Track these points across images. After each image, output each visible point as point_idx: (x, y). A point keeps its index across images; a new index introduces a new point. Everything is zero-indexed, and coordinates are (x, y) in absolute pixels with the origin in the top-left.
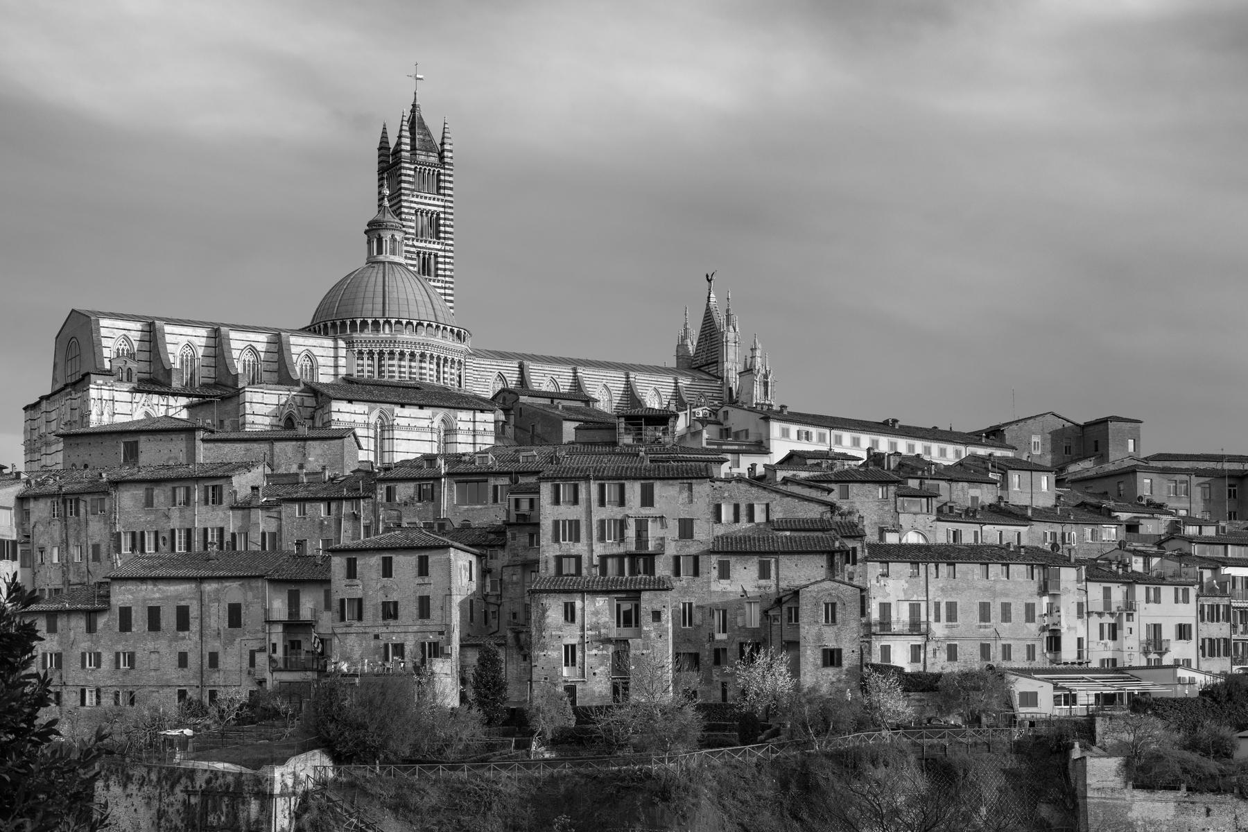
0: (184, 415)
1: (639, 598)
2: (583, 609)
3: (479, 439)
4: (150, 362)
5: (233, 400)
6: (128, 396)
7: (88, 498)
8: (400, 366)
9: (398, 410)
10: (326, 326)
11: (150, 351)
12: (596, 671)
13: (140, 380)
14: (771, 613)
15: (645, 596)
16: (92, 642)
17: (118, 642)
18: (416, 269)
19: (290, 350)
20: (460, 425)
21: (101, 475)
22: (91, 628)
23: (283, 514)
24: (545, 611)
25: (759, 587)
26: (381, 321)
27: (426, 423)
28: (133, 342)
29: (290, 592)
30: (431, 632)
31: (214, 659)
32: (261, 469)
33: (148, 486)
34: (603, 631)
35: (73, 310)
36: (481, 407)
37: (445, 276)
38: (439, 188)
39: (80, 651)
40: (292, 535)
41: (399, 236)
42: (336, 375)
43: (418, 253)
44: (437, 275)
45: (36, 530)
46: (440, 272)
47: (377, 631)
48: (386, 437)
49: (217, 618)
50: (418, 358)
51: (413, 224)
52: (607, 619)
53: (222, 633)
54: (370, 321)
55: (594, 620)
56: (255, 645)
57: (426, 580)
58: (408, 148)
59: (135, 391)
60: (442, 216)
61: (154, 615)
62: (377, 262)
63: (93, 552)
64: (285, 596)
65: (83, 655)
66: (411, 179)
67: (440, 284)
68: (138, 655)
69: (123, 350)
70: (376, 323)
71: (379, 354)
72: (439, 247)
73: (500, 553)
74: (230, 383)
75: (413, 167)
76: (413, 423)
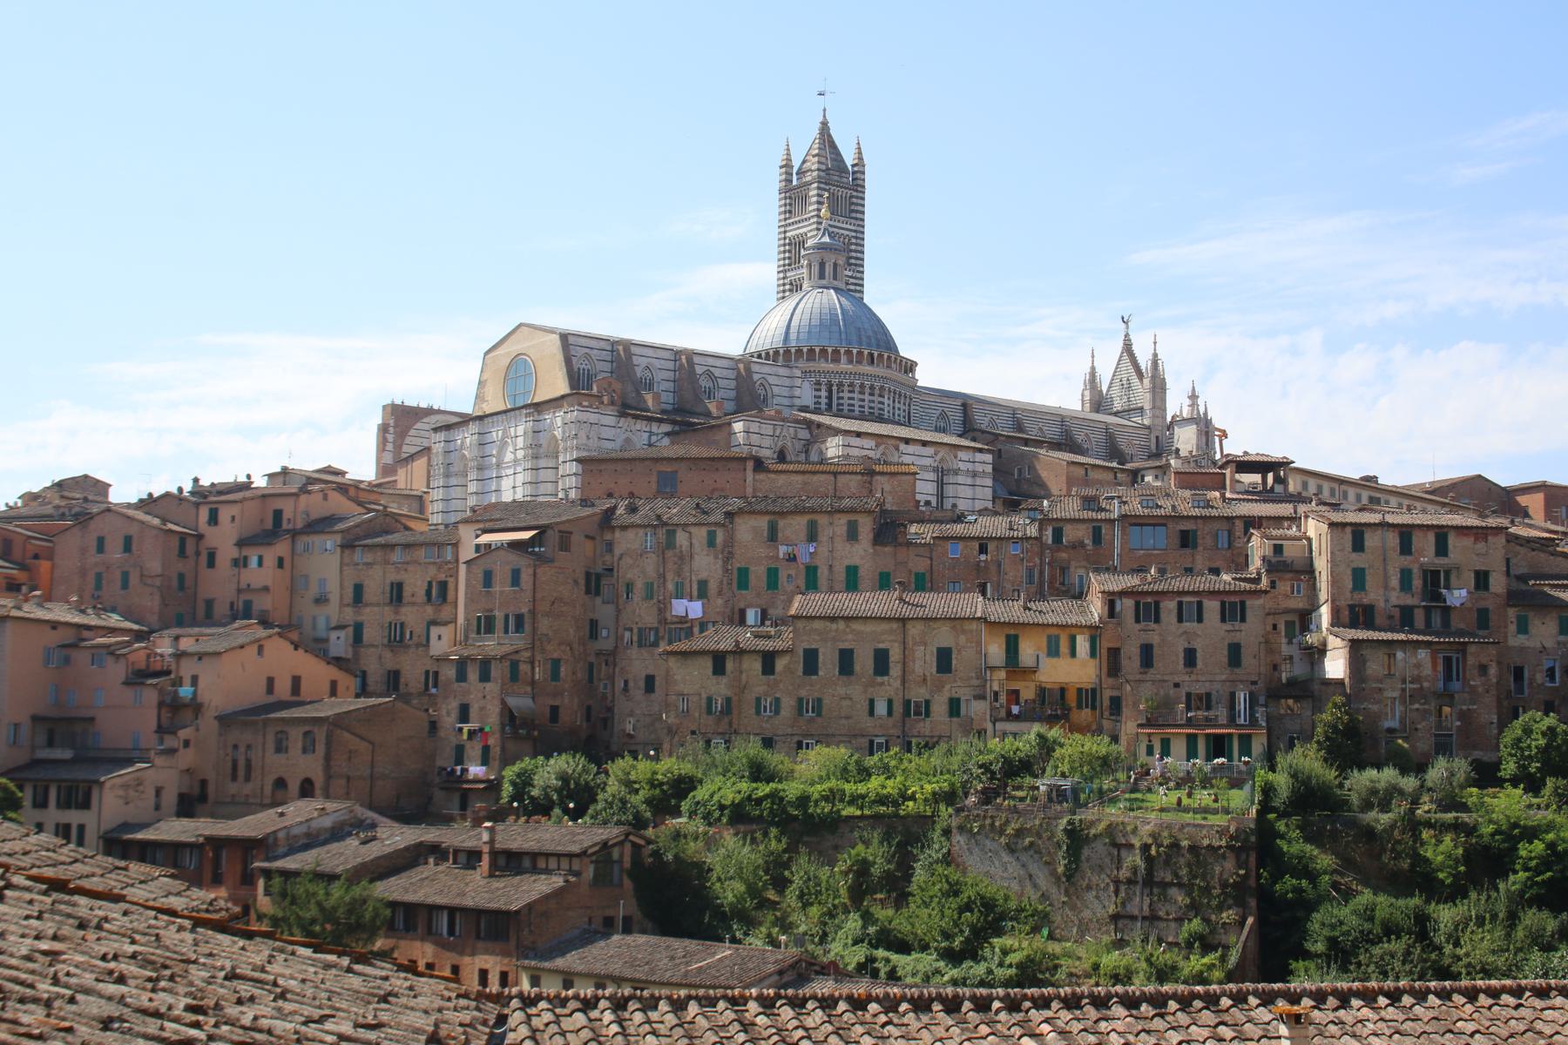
1: (1464, 652)
6: (611, 420)
7: (693, 530)
9: (902, 447)
15: (1472, 649)
24: (1364, 662)
27: (928, 462)
29: (1008, 637)
30: (1241, 681)
33: (772, 517)
35: (520, 325)
47: (1177, 680)
49: (924, 661)
50: (877, 392)
55: (1416, 672)
59: (623, 415)
61: (846, 661)
63: (699, 589)
64: (1003, 640)
65: (758, 700)
68: (826, 701)
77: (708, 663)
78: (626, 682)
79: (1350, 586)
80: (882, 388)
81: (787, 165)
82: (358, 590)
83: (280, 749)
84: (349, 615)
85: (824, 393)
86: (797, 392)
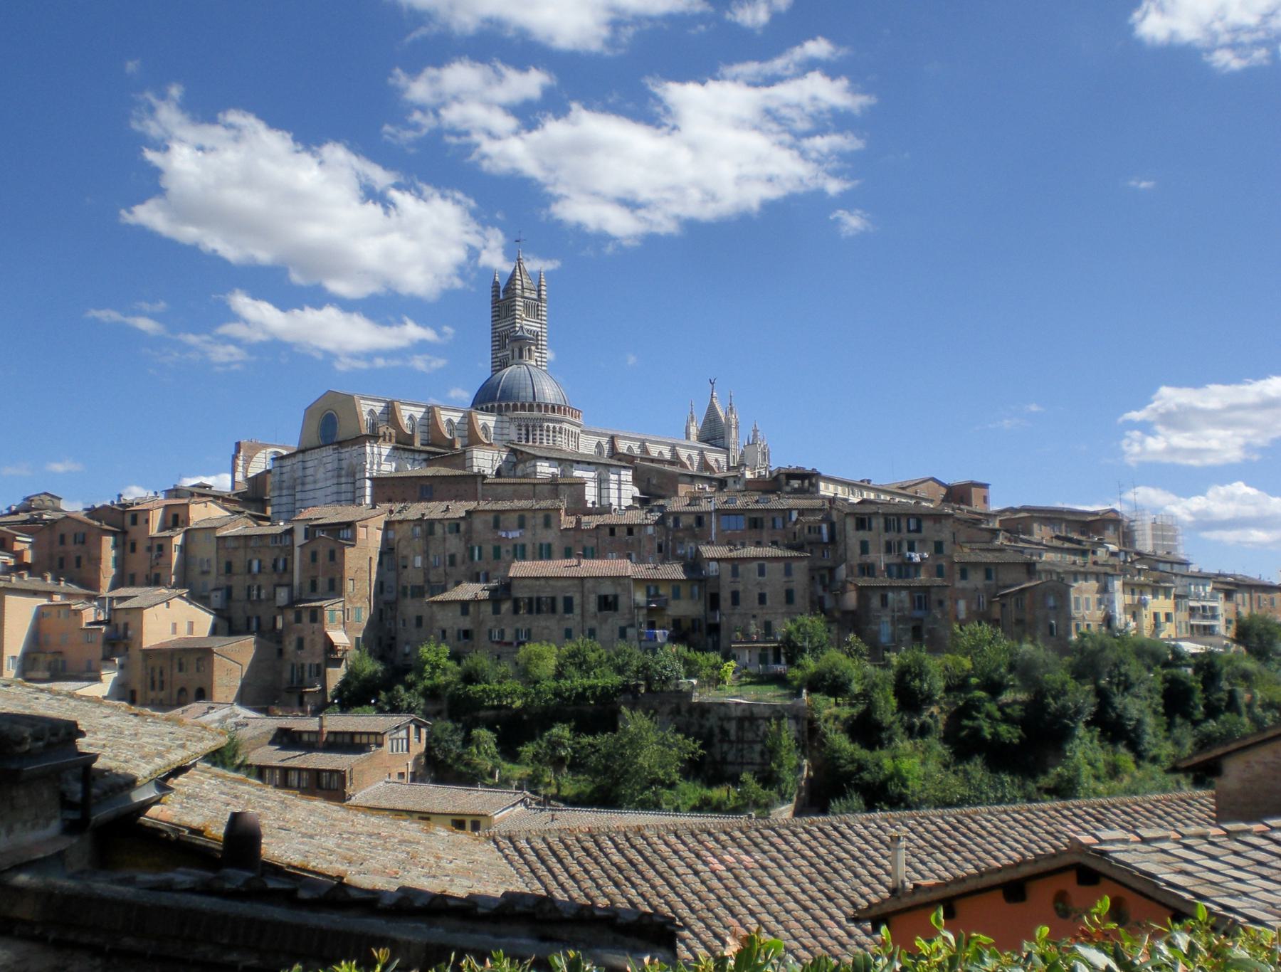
45: (401, 544)
47: (755, 612)
77: (458, 608)
78: (404, 620)
81: (496, 286)
82: (229, 566)
83: (181, 670)
84: (223, 581)
85: (523, 432)
86: (506, 431)
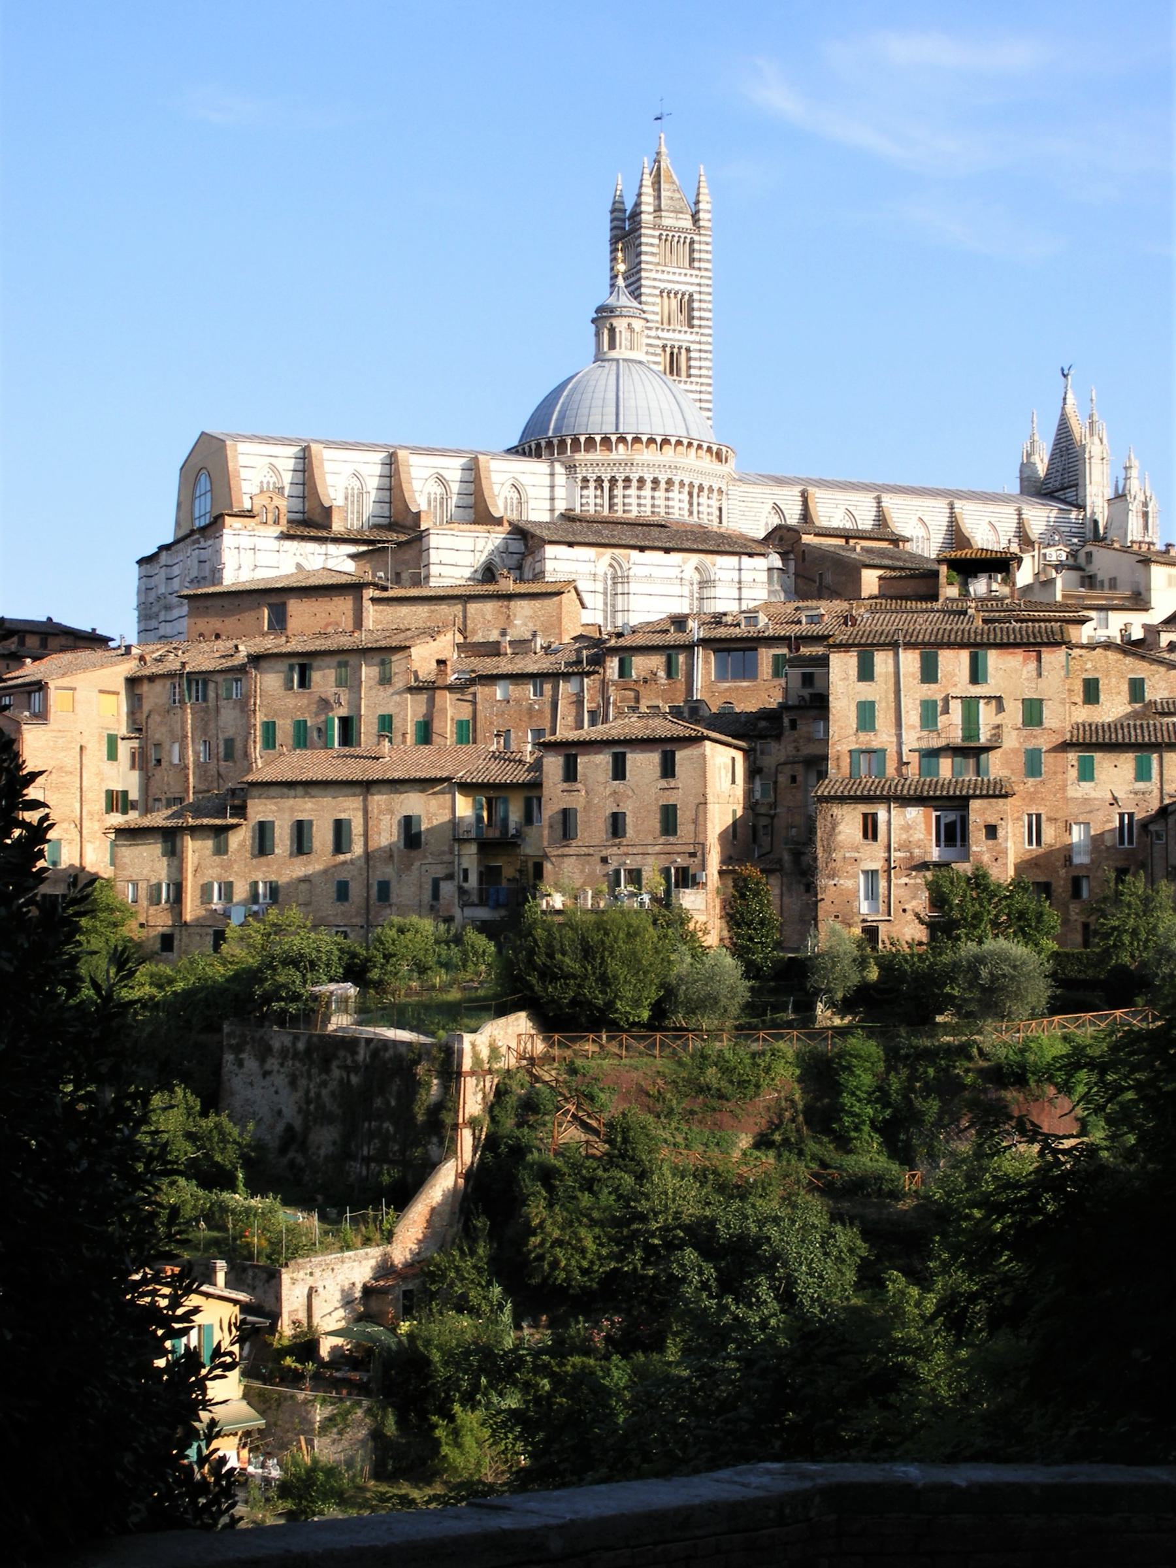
0: (350, 566)
1: (966, 807)
2: (889, 823)
3: (746, 593)
4: (304, 497)
5: (414, 545)
7: (220, 678)
8: (639, 497)
9: (635, 554)
10: (538, 445)
11: (304, 484)
12: (906, 907)
13: (290, 521)
14: (1152, 828)
15: (974, 804)
16: (222, 867)
17: (256, 868)
18: (661, 368)
19: (489, 478)
20: (721, 575)
21: (236, 647)
22: (221, 850)
23: (479, 696)
24: (834, 825)
25: (1136, 793)
26: (614, 438)
28: (282, 473)
30: (679, 853)
31: (384, 890)
32: (449, 636)
34: (917, 852)
35: (203, 434)
36: (749, 550)
37: (700, 376)
38: (692, 260)
39: (206, 880)
40: (491, 723)
41: (638, 324)
42: (552, 510)
43: (664, 347)
44: (689, 376)
45: (150, 721)
46: (693, 371)
47: (604, 853)
48: (619, 591)
50: (663, 486)
51: (657, 309)
52: (922, 836)
53: (395, 855)
54: (598, 438)
55: (904, 836)
56: (439, 871)
57: (673, 783)
58: (651, 209)
60: (696, 296)
62: (609, 360)
63: (226, 748)
66: (654, 250)
67: (694, 387)
69: (268, 483)
70: (606, 441)
71: (610, 481)
72: (694, 338)
73: (773, 746)
74: (409, 522)
75: (657, 233)
76: (657, 572)
79: (855, 726)
80: (670, 482)
